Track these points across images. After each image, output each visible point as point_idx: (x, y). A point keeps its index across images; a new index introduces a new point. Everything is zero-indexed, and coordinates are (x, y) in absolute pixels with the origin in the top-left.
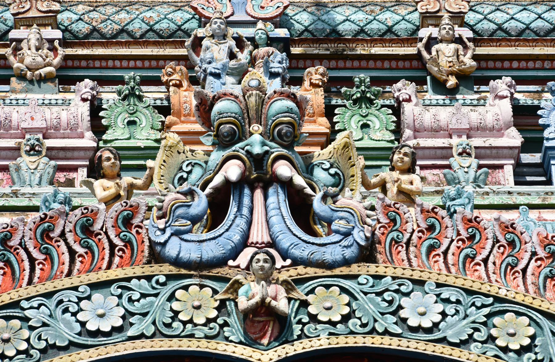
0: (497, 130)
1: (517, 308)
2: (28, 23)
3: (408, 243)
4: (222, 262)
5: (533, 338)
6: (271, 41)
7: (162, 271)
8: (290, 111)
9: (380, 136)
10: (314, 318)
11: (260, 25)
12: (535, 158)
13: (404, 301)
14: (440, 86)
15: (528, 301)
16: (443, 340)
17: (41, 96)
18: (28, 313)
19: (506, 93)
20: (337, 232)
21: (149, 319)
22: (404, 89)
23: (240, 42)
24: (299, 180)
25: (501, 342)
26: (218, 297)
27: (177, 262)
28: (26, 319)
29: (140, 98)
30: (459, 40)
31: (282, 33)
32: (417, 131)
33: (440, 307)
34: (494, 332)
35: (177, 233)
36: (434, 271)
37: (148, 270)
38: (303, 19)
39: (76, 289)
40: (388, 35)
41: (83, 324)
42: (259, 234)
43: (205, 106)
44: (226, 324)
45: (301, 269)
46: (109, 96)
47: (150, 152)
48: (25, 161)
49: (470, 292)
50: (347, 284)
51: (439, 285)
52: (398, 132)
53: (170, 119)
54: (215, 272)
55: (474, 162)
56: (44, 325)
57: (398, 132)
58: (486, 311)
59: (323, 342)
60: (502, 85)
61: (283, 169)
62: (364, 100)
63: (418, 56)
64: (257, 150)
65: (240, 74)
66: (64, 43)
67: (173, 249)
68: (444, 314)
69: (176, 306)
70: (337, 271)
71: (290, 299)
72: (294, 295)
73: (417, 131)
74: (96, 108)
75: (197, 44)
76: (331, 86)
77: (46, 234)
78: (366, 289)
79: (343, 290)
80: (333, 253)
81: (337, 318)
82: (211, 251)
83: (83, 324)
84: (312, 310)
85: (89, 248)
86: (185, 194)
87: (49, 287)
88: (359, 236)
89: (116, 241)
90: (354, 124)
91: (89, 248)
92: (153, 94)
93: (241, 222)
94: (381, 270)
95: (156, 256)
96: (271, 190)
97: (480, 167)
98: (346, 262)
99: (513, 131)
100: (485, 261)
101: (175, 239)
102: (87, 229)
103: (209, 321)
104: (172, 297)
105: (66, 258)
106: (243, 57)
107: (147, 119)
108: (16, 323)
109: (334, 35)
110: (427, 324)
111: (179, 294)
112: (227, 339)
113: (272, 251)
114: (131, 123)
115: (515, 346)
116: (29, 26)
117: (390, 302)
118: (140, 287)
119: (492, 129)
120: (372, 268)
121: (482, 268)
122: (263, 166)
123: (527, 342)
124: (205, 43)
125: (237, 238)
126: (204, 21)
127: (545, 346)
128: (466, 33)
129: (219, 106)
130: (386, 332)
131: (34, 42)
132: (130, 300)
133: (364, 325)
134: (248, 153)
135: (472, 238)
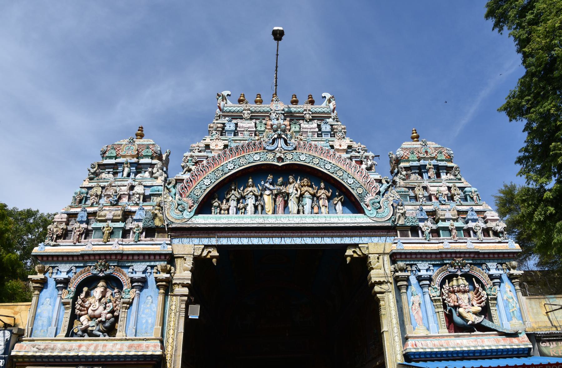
0: (315, 129)
2: (246, 110)
6: (282, 113)
7: (265, 151)
9: (297, 129)
12: (320, 132)
14: (306, 121)
22: (301, 122)
27: (267, 150)
32: (303, 128)
36: (305, 152)
38: (286, 110)
40: (299, 112)
42: (279, 146)
43: (272, 126)
46: (257, 122)
47: (264, 131)
48: (245, 132)
52: (300, 128)
57: (300, 128)
59: (288, 162)
60: (316, 121)
61: (283, 136)
62: (295, 123)
65: (278, 119)
67: (267, 148)
73: (303, 128)
74: (256, 124)
75: (271, 114)
76: (290, 121)
80: (290, 149)
82: (272, 148)
88: (294, 146)
90: (294, 127)
92: (264, 122)
95: (264, 149)
102: (254, 145)
106: (277, 116)
109: (291, 112)
122: (281, 134)
126: (272, 110)
128: (310, 113)
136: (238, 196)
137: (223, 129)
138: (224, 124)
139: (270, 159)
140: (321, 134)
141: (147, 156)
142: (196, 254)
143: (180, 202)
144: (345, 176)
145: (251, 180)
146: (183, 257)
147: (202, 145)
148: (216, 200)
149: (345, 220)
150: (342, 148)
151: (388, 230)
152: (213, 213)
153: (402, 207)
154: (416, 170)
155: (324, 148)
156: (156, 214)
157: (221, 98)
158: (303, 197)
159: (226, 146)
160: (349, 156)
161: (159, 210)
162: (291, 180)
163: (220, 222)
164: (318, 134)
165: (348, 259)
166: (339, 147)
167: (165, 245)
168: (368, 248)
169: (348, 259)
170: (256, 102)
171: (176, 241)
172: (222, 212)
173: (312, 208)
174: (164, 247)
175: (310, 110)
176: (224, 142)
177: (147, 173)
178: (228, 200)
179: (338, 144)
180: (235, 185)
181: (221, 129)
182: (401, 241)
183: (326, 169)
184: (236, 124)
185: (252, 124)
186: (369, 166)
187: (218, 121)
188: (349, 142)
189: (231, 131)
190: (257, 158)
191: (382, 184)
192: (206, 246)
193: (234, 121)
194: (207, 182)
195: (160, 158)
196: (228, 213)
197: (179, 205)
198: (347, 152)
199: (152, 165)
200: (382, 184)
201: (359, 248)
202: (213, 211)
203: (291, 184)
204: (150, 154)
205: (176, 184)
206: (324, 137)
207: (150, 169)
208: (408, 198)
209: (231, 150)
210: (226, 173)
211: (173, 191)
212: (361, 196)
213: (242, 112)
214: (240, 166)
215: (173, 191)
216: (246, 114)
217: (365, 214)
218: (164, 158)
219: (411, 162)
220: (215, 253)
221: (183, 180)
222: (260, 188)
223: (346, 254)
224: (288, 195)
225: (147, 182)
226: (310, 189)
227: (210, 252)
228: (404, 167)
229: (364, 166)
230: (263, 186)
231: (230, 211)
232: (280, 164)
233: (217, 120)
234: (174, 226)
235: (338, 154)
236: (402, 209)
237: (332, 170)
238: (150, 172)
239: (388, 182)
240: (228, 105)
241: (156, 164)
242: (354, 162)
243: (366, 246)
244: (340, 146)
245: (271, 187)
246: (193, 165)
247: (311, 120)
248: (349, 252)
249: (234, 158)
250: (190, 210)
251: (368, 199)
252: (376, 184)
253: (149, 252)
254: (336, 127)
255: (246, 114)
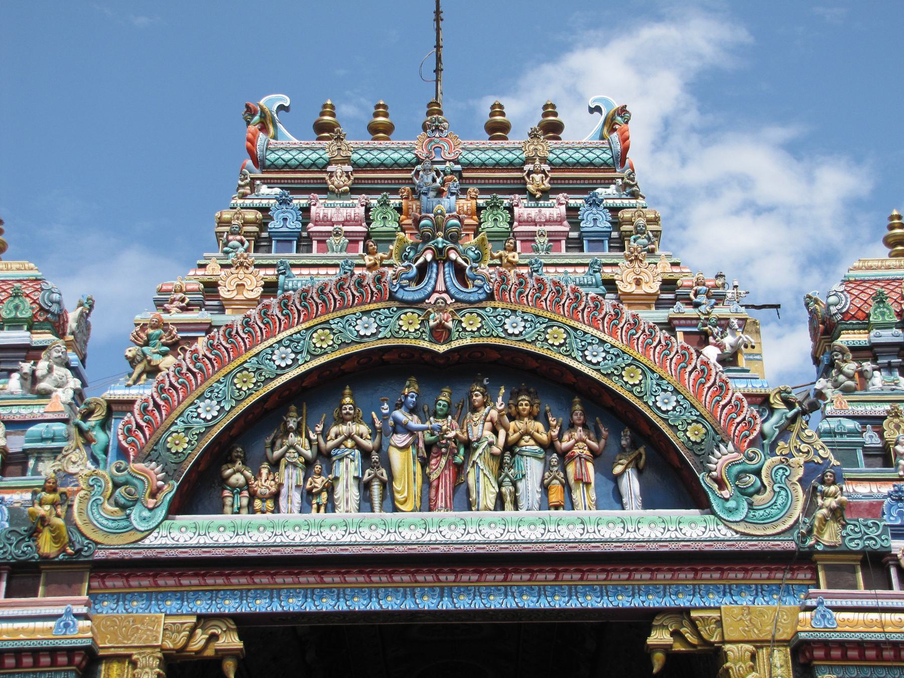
1: (559, 324)
2: (337, 162)
3: (510, 291)
4: (422, 301)
5: (565, 339)
7: (394, 305)
8: (456, 225)
9: (503, 225)
10: (464, 329)
11: (448, 164)
13: (507, 321)
14: (532, 197)
15: (564, 320)
16: (524, 340)
17: (341, 202)
18: (333, 326)
19: (564, 202)
20: (476, 286)
21: (388, 329)
23: (438, 174)
24: (460, 260)
25: (550, 342)
26: (421, 318)
27: (402, 301)
28: (331, 329)
29: (388, 205)
30: (543, 172)
31: (458, 167)
33: (523, 324)
34: (547, 336)
35: (402, 287)
37: (389, 304)
39: (355, 314)
41: (358, 332)
42: (441, 287)
44: (424, 332)
45: (459, 305)
47: (392, 234)
49: (537, 316)
50: (480, 311)
51: (523, 312)
52: (511, 224)
53: (403, 217)
54: (419, 306)
55: (546, 239)
56: (340, 332)
58: (545, 325)
59: (468, 341)
60: (561, 196)
61: (453, 255)
63: (523, 178)
64: (440, 246)
66: (355, 171)
67: (400, 295)
68: (525, 327)
69: (401, 323)
70: (476, 306)
71: (453, 320)
72: (456, 318)
73: (521, 223)
77: (341, 286)
78: (489, 314)
79: (479, 315)
81: (475, 329)
82: (417, 296)
83: (358, 332)
84: (464, 325)
85: (361, 293)
86: (405, 267)
87: (343, 312)
89: (374, 289)
91: (361, 293)
92: (395, 201)
93: (433, 282)
94: (496, 305)
95: (392, 297)
96: (446, 265)
97: (550, 241)
98: (480, 301)
99: (566, 223)
100: (546, 299)
101: (401, 290)
103: (416, 330)
104: (399, 318)
105: (351, 298)
107: (392, 215)
108: (327, 331)
110: (517, 332)
111: (402, 316)
112: (424, 339)
113: (445, 296)
114: (385, 218)
115: (557, 344)
116: (337, 164)
117: (500, 321)
118: (384, 313)
119: (556, 221)
120: (493, 304)
121: (544, 303)
123: (562, 341)
124: (421, 173)
125: (430, 289)
127: (570, 344)
128: (547, 168)
129: (424, 222)
130: (498, 336)
131: (339, 174)
132: (380, 320)
133: (487, 333)
134: (436, 247)
135: (540, 288)
136: (309, 453)
137: (263, 225)
138: (264, 210)
139: (409, 330)
140: (580, 240)
141: (15, 324)
142: (169, 645)
143: (121, 477)
144: (651, 382)
145: (348, 400)
146: (129, 656)
147: (192, 280)
148: (238, 465)
149: (646, 532)
150: (645, 289)
151: (792, 563)
152: (228, 509)
153: (833, 488)
154: (890, 354)
155: (583, 290)
156: (43, 519)
157: (257, 118)
158: (513, 455)
159: (270, 288)
160: (663, 315)
161: (54, 504)
162: (478, 398)
163: (247, 540)
164: (569, 240)
165: (658, 660)
166: (631, 288)
167: (70, 620)
168: (719, 622)
169: (658, 660)
170: (374, 129)
171: (107, 607)
172: (258, 503)
173: (545, 488)
174: (67, 626)
175: (544, 160)
176: (262, 272)
177: (16, 376)
178: (275, 465)
179: (631, 278)
180: (300, 414)
181: (255, 229)
182: (828, 602)
183: (589, 362)
184: (306, 210)
185: (355, 207)
186: (728, 350)
187: (248, 202)
188: (669, 269)
189: (290, 234)
190: (368, 330)
191: (772, 411)
192: (203, 619)
193: (300, 201)
194: (208, 409)
195: (58, 326)
196: (277, 509)
197: (116, 486)
198: (660, 304)
199: (32, 352)
200: (772, 411)
201: (693, 623)
202: (228, 501)
203: (475, 410)
204: (27, 314)
205: (110, 412)
206: (588, 255)
207: (26, 367)
208: (860, 453)
209: (284, 305)
210: (268, 380)
211: (100, 436)
212: (702, 451)
213: (323, 168)
214: (314, 357)
215: (100, 436)
216: (339, 176)
217: (713, 513)
218: (72, 324)
219: (874, 332)
220: (231, 641)
221: (132, 402)
222: (378, 424)
223: (650, 641)
224: (469, 446)
225: (15, 410)
226: (539, 425)
227: (214, 637)
228: (853, 349)
229: (711, 353)
230: (384, 418)
231: (282, 502)
232: (441, 349)
233: (243, 196)
234: (100, 555)
235: (627, 312)
236: (834, 496)
237: (608, 366)
238: (24, 377)
239: (790, 404)
240: (280, 143)
241: (44, 348)
242: (680, 336)
243: (715, 614)
244: (638, 282)
245: (414, 422)
246: (164, 354)
247: (546, 194)
248: (659, 637)
249: (295, 329)
250: (151, 503)
251: (723, 459)
252: (748, 411)
253: (18, 645)
254: (626, 214)
255: (339, 176)
